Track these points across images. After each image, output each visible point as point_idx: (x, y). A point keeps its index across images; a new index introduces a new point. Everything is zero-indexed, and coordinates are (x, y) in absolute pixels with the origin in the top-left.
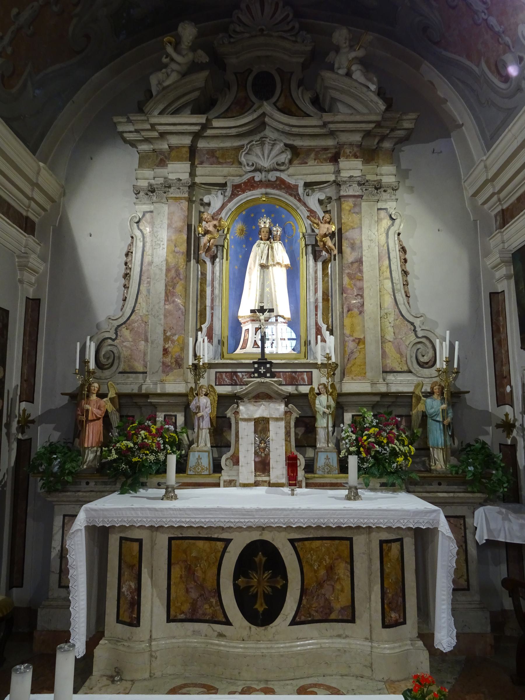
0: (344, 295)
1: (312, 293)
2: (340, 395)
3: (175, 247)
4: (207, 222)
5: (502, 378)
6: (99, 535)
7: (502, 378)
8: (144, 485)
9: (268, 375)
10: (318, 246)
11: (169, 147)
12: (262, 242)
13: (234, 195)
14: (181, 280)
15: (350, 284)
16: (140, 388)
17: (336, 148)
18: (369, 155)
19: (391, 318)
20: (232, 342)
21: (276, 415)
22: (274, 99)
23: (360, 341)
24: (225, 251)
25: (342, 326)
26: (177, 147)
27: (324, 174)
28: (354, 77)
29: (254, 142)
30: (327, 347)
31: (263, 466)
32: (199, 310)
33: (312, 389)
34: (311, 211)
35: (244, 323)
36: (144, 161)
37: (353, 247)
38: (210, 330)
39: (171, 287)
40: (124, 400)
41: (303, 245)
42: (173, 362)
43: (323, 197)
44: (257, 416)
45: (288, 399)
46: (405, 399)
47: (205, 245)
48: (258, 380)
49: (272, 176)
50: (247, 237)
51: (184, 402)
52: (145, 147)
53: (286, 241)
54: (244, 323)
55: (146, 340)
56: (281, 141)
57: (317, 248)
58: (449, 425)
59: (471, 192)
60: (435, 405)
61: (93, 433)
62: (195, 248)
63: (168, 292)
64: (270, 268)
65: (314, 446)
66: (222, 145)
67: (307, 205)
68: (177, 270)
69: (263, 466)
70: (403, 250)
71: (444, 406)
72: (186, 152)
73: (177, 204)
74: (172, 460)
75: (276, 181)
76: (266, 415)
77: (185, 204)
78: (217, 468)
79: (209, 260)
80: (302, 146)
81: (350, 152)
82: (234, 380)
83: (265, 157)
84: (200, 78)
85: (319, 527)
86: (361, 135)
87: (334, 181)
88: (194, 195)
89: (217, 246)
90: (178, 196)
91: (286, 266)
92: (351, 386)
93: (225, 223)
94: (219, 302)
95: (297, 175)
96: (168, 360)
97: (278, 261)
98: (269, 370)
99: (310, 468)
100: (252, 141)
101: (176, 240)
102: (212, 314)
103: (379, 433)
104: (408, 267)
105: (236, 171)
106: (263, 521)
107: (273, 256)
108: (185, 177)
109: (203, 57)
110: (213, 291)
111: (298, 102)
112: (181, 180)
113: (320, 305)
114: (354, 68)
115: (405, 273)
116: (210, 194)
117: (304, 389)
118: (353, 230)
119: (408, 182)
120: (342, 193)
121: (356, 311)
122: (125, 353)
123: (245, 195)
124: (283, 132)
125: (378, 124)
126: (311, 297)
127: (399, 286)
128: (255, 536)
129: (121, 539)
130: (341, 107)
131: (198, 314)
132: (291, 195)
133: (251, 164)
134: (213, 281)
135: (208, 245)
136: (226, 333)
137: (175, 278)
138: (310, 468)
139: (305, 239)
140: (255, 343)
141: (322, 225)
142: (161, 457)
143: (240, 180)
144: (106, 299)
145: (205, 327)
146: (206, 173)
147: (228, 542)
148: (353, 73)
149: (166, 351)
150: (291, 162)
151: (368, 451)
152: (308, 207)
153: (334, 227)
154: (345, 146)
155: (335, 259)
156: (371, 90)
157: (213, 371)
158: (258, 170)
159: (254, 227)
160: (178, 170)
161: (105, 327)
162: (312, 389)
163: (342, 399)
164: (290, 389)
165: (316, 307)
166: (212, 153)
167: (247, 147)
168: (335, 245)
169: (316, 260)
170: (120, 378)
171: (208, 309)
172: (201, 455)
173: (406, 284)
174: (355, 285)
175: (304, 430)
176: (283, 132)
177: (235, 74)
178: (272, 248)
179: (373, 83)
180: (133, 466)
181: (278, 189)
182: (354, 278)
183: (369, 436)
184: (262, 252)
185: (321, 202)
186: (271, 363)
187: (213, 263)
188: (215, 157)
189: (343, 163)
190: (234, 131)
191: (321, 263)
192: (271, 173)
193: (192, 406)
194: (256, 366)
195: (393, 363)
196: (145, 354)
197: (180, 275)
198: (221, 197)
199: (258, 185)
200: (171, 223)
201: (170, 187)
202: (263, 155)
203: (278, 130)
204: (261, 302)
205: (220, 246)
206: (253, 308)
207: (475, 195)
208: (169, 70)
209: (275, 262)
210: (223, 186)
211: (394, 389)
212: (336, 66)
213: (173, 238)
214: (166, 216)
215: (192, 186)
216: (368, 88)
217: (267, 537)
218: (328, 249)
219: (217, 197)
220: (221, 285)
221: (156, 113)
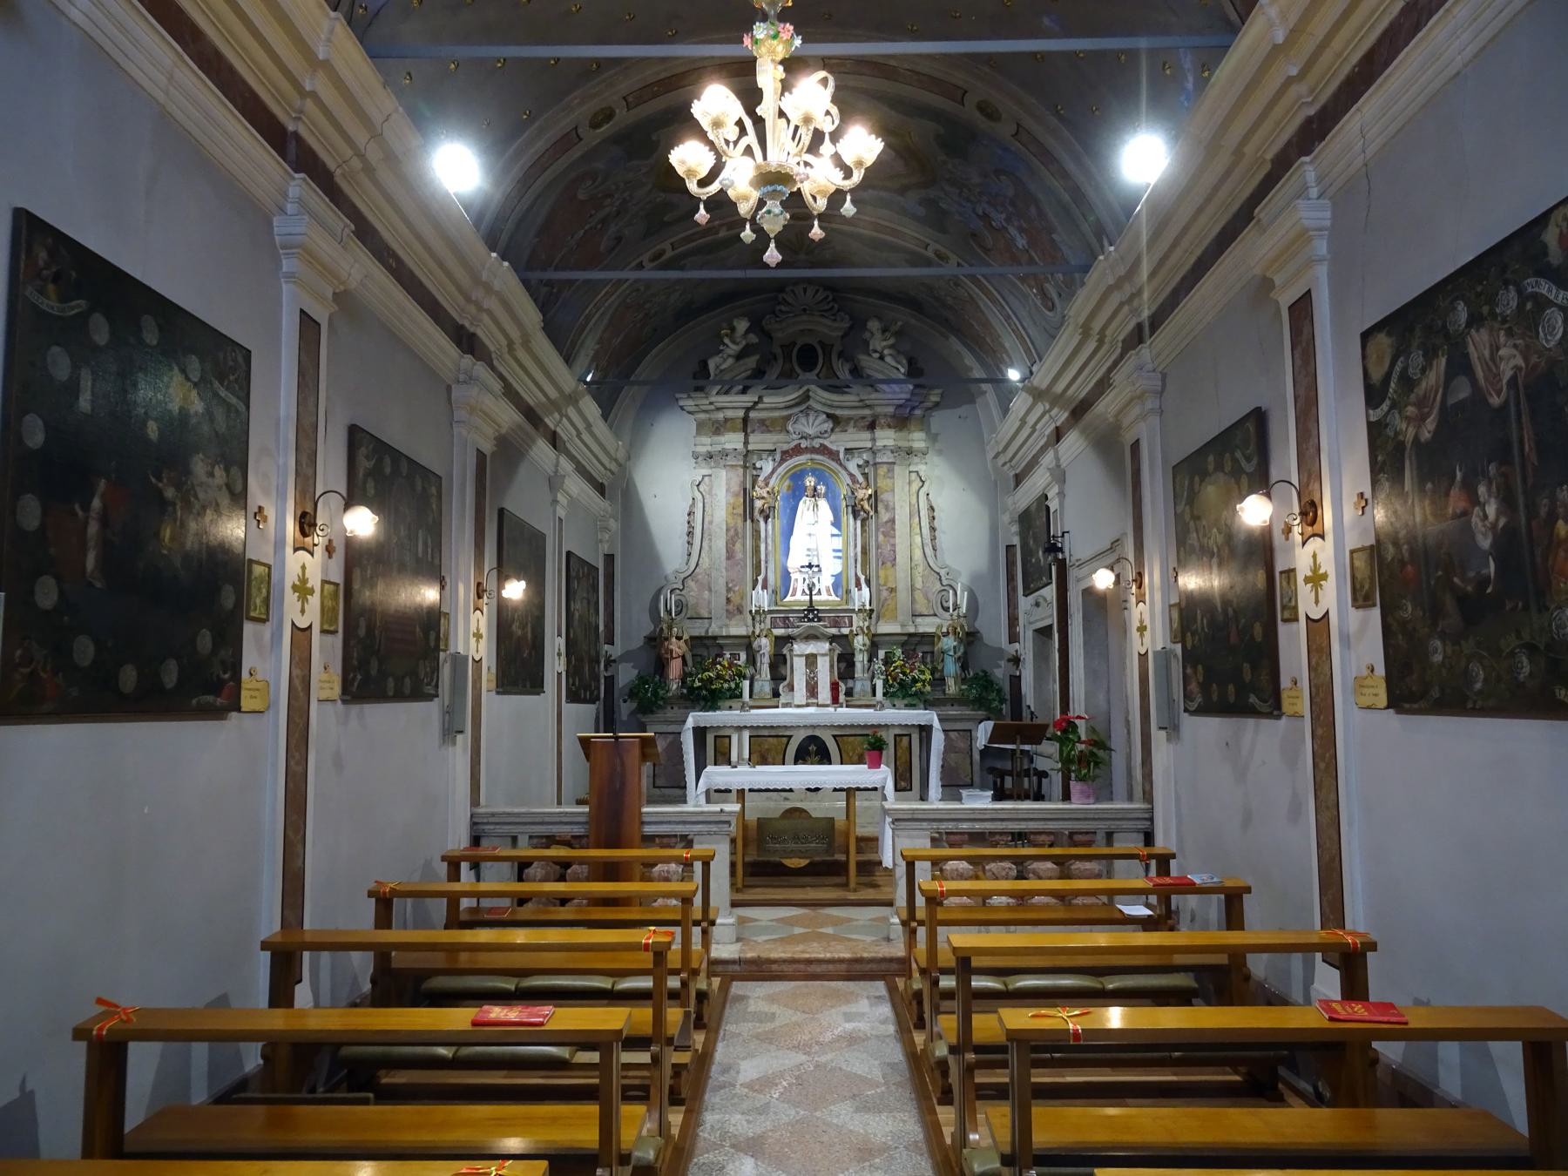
5: (1013, 621)
6: (700, 733)
7: (1013, 621)
8: (719, 708)
13: (783, 461)
18: (901, 421)
19: (920, 569)
23: (893, 590)
30: (862, 597)
31: (812, 690)
34: (851, 475)
37: (886, 508)
38: (765, 580)
40: (696, 642)
42: (735, 609)
45: (833, 639)
46: (929, 639)
49: (816, 443)
51: (747, 643)
52: (702, 416)
60: (949, 643)
61: (675, 669)
62: (749, 510)
69: (812, 690)
70: (932, 509)
74: (747, 683)
77: (741, 471)
78: (776, 694)
83: (812, 426)
84: (752, 362)
85: (852, 726)
92: (884, 628)
95: (838, 442)
96: (731, 607)
99: (849, 693)
106: (814, 722)
108: (740, 446)
109: (753, 339)
114: (886, 352)
117: (845, 631)
119: (938, 446)
122: (692, 601)
127: (928, 541)
128: (810, 732)
138: (849, 693)
144: (672, 553)
145: (760, 578)
146: (758, 441)
151: (894, 679)
160: (733, 441)
161: (672, 578)
164: (834, 631)
166: (762, 422)
170: (688, 623)
172: (764, 683)
173: (933, 539)
180: (713, 692)
188: (765, 426)
189: (879, 433)
193: (755, 645)
195: (921, 607)
207: (996, 457)
211: (921, 630)
217: (818, 733)
218: (863, 512)
220: (774, 541)
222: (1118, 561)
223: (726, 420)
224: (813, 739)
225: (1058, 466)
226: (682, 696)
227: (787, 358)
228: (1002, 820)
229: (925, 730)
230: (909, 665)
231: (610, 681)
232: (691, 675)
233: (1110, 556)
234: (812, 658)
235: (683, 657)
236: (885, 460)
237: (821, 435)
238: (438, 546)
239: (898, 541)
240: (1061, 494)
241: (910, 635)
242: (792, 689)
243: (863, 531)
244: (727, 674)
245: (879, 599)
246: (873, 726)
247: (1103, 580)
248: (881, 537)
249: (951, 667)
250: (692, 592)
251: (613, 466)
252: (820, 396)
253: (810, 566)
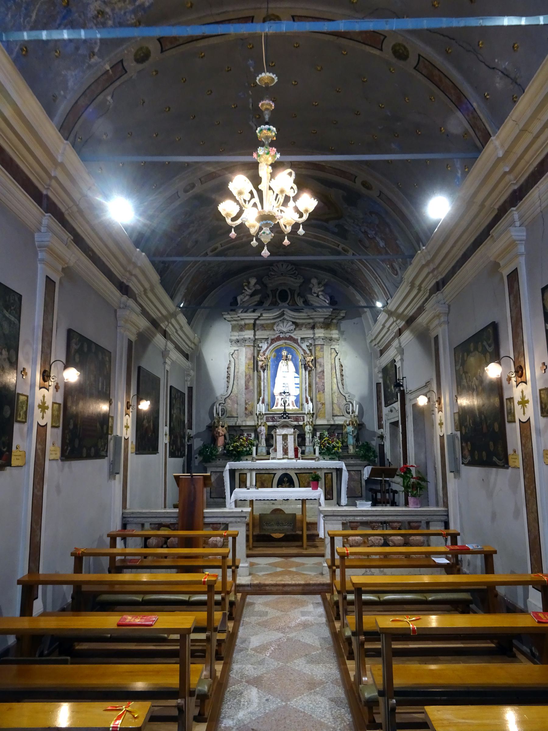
1: (304, 384)
2: (314, 425)
5: (380, 418)
7: (380, 418)
8: (241, 460)
13: (272, 343)
16: (236, 423)
18: (327, 325)
19: (336, 394)
20: (272, 404)
21: (290, 433)
22: (288, 302)
23: (323, 404)
25: (316, 397)
30: (309, 407)
31: (285, 451)
33: (304, 423)
34: (303, 350)
36: (234, 328)
37: (320, 365)
38: (263, 399)
42: (249, 413)
43: (308, 344)
44: (283, 433)
45: (295, 427)
46: (341, 427)
49: (287, 335)
51: (255, 429)
52: (234, 323)
55: (237, 404)
58: (355, 436)
59: (370, 341)
60: (350, 429)
61: (221, 441)
62: (256, 366)
65: (305, 445)
68: (250, 376)
69: (285, 451)
71: (353, 429)
74: (254, 449)
76: (286, 433)
77: (252, 348)
78: (268, 453)
83: (285, 327)
84: (257, 298)
92: (319, 422)
95: (297, 335)
96: (247, 412)
98: (287, 416)
99: (303, 453)
103: (329, 440)
104: (343, 373)
106: (287, 467)
108: (252, 337)
109: (258, 287)
113: (307, 389)
114: (320, 293)
115: (342, 375)
117: (301, 423)
119: (344, 337)
120: (316, 343)
121: (321, 392)
122: (229, 409)
125: (330, 315)
127: (340, 381)
128: (284, 472)
129: (240, 474)
138: (303, 453)
142: (248, 449)
144: (220, 386)
145: (261, 398)
146: (260, 334)
147: (275, 474)
149: (246, 409)
150: (295, 329)
151: (324, 446)
157: (265, 416)
160: (249, 334)
161: (219, 398)
162: (304, 423)
163: (315, 427)
164: (296, 423)
166: (262, 325)
169: (305, 370)
170: (227, 420)
171: (262, 391)
172: (263, 447)
173: (342, 380)
175: (301, 439)
177: (271, 291)
183: (325, 441)
188: (264, 327)
189: (316, 331)
193: (258, 430)
195: (336, 412)
196: (237, 410)
207: (371, 342)
211: (337, 423)
215: (255, 340)
217: (288, 472)
218: (309, 367)
220: (267, 381)
221: (240, 311)
222: (429, 391)
223: (245, 324)
224: (286, 475)
225: (400, 346)
226: (224, 454)
227: (274, 296)
228: (376, 516)
229: (339, 471)
230: (331, 440)
231: (190, 447)
232: (228, 444)
233: (425, 389)
234: (285, 436)
235: (225, 436)
236: (320, 343)
238: (109, 385)
239: (325, 381)
240: (402, 360)
241: (332, 425)
242: (275, 450)
243: (309, 376)
244: (245, 444)
245: (317, 408)
246: (314, 469)
247: (422, 401)
248: (318, 379)
249: (351, 441)
250: (229, 404)
251: (192, 346)
252: (289, 314)
253: (284, 393)
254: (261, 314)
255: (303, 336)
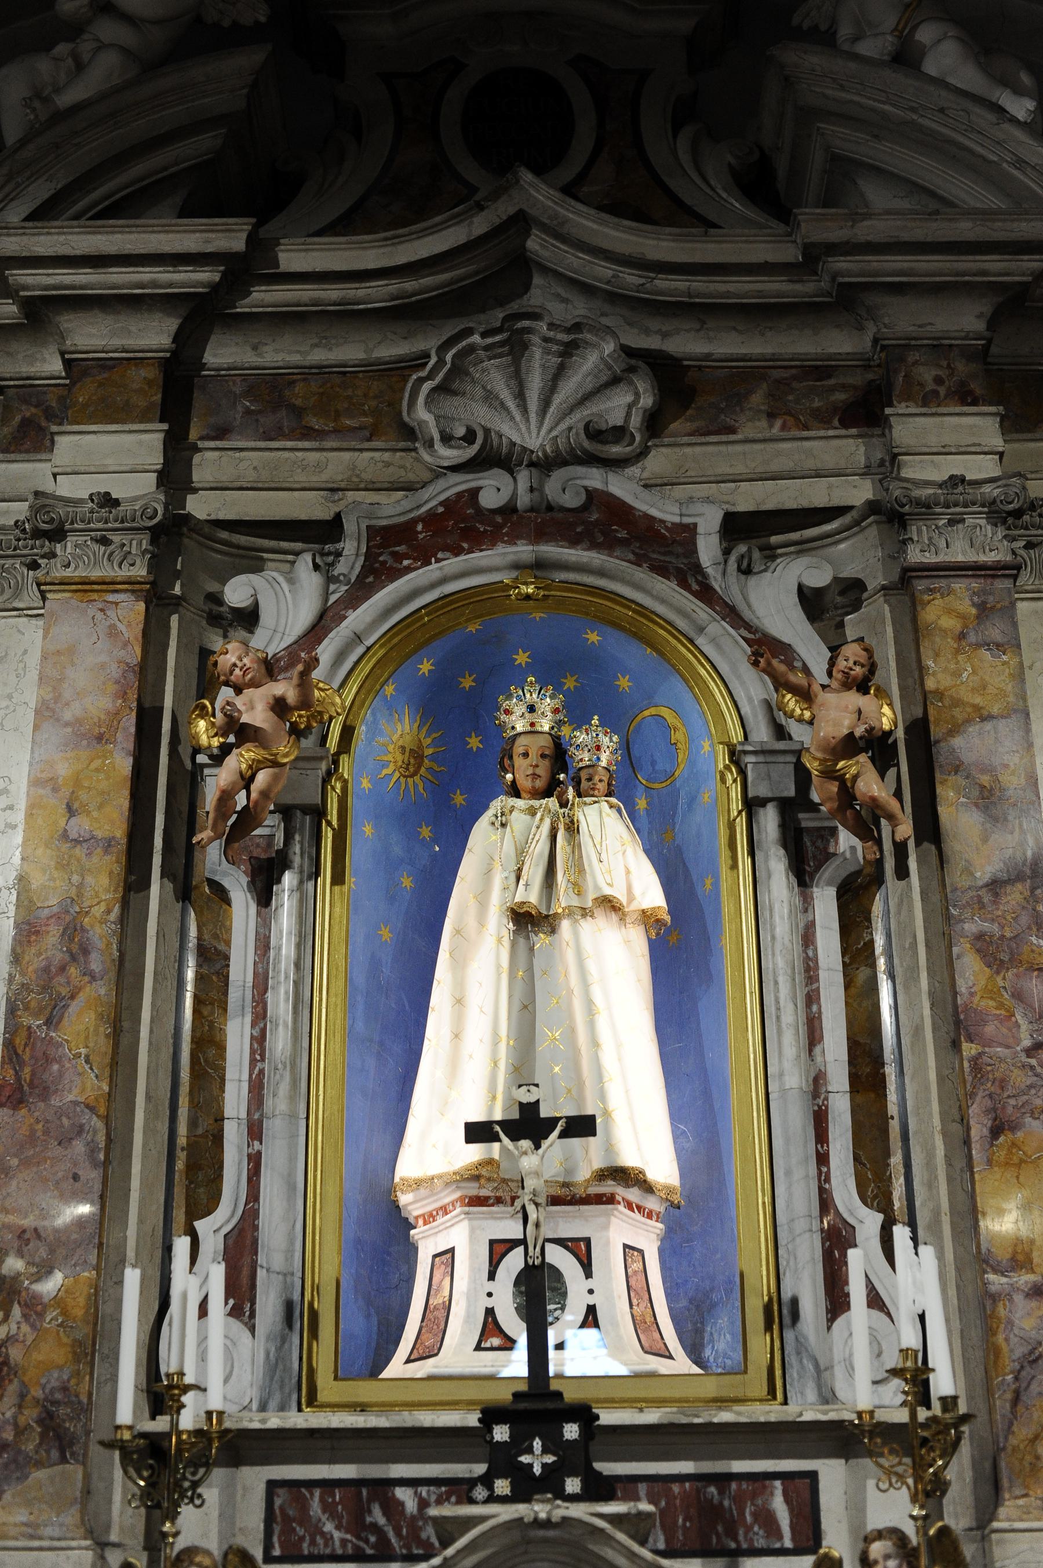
0: (969, 1049)
1: (788, 1045)
3: (71, 812)
4: (238, 690)
9: (573, 1485)
10: (814, 808)
11: (68, 364)
12: (520, 803)
13: (375, 573)
14: (93, 978)
15: (991, 992)
17: (867, 367)
20: (358, 1322)
24: (328, 836)
26: (106, 365)
27: (818, 474)
28: (930, 67)
29: (476, 338)
32: (182, 1141)
35: (429, 1218)
37: (988, 799)
39: (36, 1015)
41: (736, 805)
43: (819, 577)
47: (226, 797)
48: (521, 1510)
49: (567, 488)
50: (440, 789)
53: (642, 804)
54: (429, 1218)
56: (609, 331)
57: (806, 821)
63: (19, 1041)
64: (565, 925)
66: (319, 356)
67: (747, 614)
68: (73, 932)
72: (150, 383)
73: (92, 610)
75: (585, 508)
77: (130, 612)
79: (244, 880)
80: (708, 357)
81: (938, 380)
82: (375, 1528)
84: (226, 78)
86: (985, 307)
87: (873, 508)
88: (177, 575)
89: (286, 812)
90: (96, 574)
91: (647, 917)
93: (336, 697)
94: (293, 1098)
95: (689, 486)
97: (608, 891)
100: (468, 332)
101: (77, 781)
102: (255, 1162)
105: (388, 464)
107: (581, 870)
108: (137, 488)
110: (259, 1040)
111: (672, 184)
112: (116, 503)
114: (925, 34)
116: (257, 568)
118: (988, 726)
120: (915, 555)
123: (431, 571)
124: (615, 298)
126: (787, 1065)
130: (876, 195)
131: (180, 1165)
132: (661, 570)
133: (461, 431)
134: (261, 985)
135: (241, 800)
136: (330, 1265)
137: (63, 969)
139: (742, 772)
140: (491, 1324)
141: (829, 699)
143: (406, 505)
148: (923, 54)
150: (655, 424)
152: (748, 627)
153: (886, 709)
154: (913, 357)
155: (902, 872)
156: (1014, 120)
157: (255, 1478)
158: (493, 457)
159: (474, 742)
165: (820, 1121)
167: (441, 362)
168: (898, 794)
169: (803, 873)
171: (233, 1135)
174: (1018, 996)
176: (615, 298)
178: (573, 828)
179: (1019, 91)
181: (594, 546)
182: (1015, 960)
184: (521, 853)
185: (812, 602)
186: (583, 1413)
187: (264, 897)
188: (284, 407)
189: (909, 426)
190: (376, 293)
191: (831, 892)
192: (559, 476)
194: (501, 1433)
197: (85, 951)
198: (309, 580)
199: (499, 527)
200: (57, 699)
201: (58, 534)
202: (520, 396)
203: (587, 289)
204: (523, 1067)
205: (306, 809)
206: (478, 1116)
208: (85, 47)
209: (591, 895)
210: (322, 534)
212: (845, 31)
213: (63, 770)
214: (34, 675)
216: (1001, 110)
219: (291, 581)
220: (303, 1004)
223: (74, 366)
236: (960, 552)
237: (599, 446)
243: (857, 953)
248: (971, 972)
252: (581, 237)
254: (260, 248)
255: (749, 498)
